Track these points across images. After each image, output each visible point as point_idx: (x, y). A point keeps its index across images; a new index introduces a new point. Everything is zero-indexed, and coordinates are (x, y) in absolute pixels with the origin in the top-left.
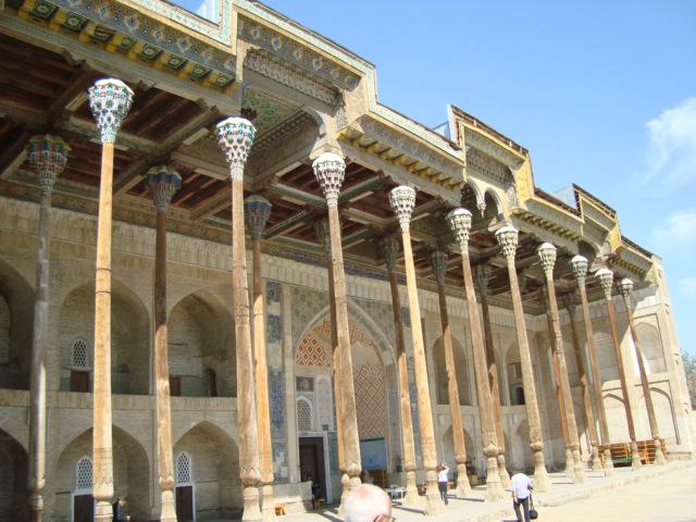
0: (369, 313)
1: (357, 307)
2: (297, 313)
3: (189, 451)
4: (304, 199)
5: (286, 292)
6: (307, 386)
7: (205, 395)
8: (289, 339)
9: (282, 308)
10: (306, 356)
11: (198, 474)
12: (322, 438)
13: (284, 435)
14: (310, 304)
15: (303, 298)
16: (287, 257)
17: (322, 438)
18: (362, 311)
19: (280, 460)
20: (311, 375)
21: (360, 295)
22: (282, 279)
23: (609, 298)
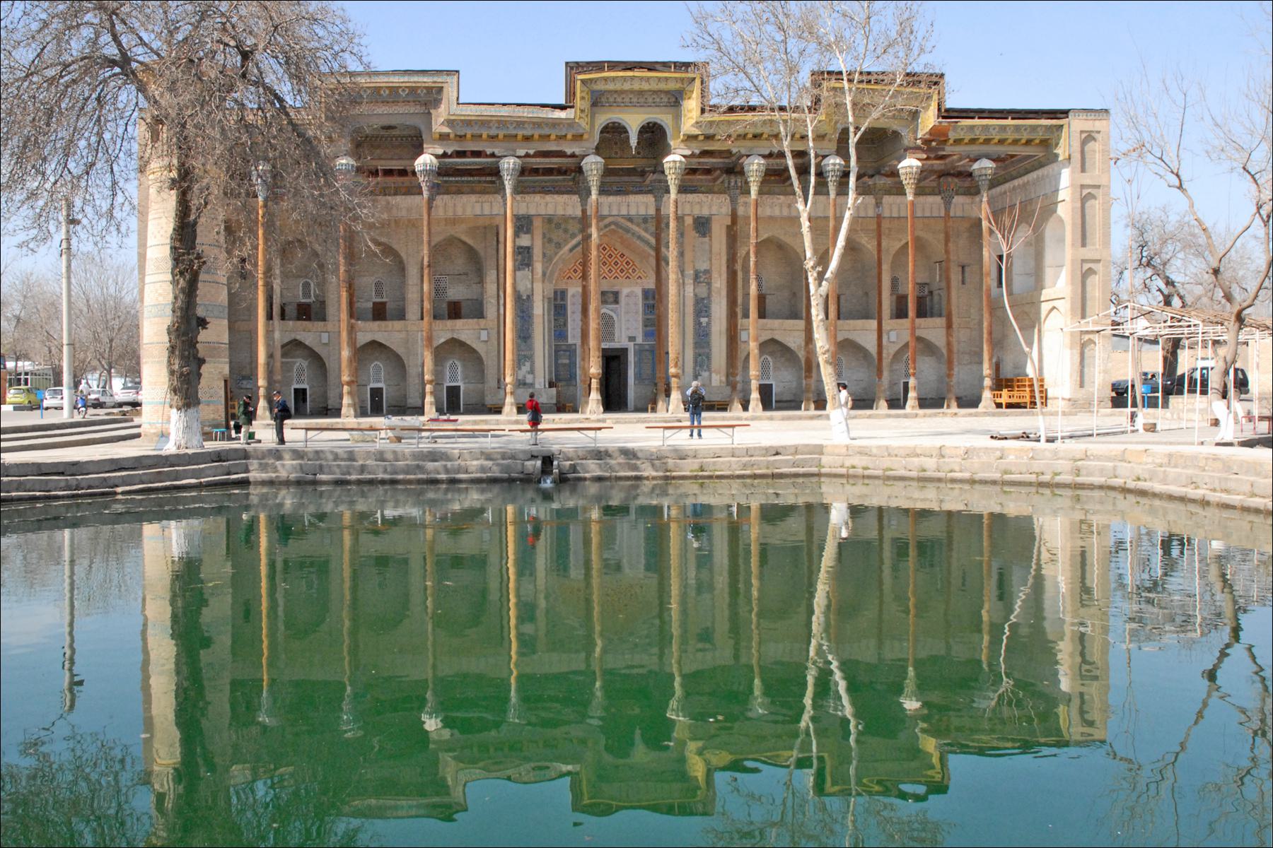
0: (646, 230)
1: (629, 224)
2: (550, 241)
3: (459, 359)
4: (480, 163)
5: (537, 223)
6: (612, 300)
7: (450, 317)
8: (538, 267)
9: (532, 239)
10: (610, 271)
11: (465, 378)
12: (626, 350)
13: (531, 348)
14: (566, 231)
15: (558, 226)
16: (534, 192)
17: (626, 350)
18: (636, 228)
19: (526, 368)
20: (615, 289)
21: (633, 212)
22: (532, 212)
23: (910, 197)
